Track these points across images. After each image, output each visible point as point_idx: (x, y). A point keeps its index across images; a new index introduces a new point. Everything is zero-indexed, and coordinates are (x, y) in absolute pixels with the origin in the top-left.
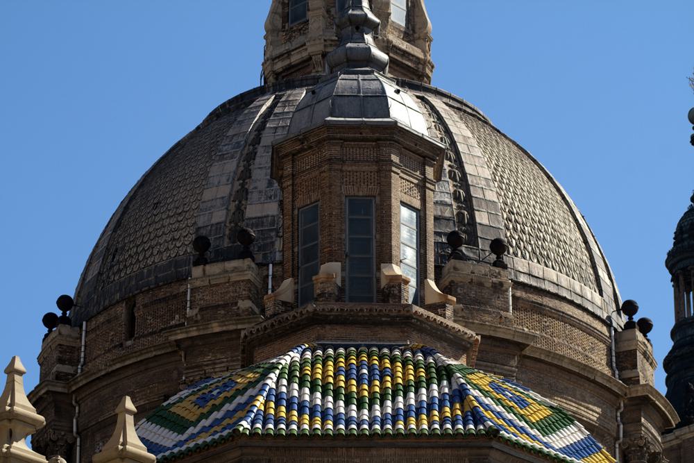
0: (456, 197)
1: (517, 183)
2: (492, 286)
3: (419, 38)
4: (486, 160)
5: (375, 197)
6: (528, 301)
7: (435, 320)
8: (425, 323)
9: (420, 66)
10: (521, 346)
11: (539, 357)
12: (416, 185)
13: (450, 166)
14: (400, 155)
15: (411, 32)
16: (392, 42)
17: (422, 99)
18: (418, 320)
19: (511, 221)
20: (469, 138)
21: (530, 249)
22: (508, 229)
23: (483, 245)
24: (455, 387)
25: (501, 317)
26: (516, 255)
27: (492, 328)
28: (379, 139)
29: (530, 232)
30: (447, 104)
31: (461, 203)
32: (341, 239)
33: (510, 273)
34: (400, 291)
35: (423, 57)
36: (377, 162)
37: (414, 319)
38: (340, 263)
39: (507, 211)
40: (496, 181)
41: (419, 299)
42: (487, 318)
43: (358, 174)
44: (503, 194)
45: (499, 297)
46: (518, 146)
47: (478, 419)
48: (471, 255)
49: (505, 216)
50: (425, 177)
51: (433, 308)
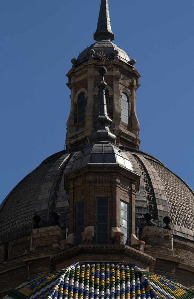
0: (149, 198)
1: (176, 192)
2: (164, 238)
3: (134, 129)
4: (162, 182)
5: (109, 197)
6: (180, 244)
7: (135, 251)
8: (130, 253)
9: (134, 141)
10: (177, 264)
11: (184, 268)
12: (128, 192)
13: (146, 185)
14: (120, 179)
15: (130, 127)
16: (122, 131)
17: (135, 155)
18: (127, 252)
19: (173, 209)
20: (155, 172)
21: (181, 221)
22: (171, 212)
23: (160, 219)
24: (143, 281)
25: (168, 251)
26: (175, 224)
27: (164, 256)
28: (111, 172)
30: (145, 158)
31: (151, 201)
32: (94, 216)
33: (172, 232)
34: (120, 239)
35: (135, 137)
36: (110, 182)
37: (126, 251)
38: (93, 227)
39: (171, 204)
40: (166, 191)
41: (128, 242)
42: (162, 251)
44: (169, 197)
45: (167, 242)
46: (177, 176)
48: (155, 224)
49: (170, 207)
50: (132, 189)
51: (135, 246)
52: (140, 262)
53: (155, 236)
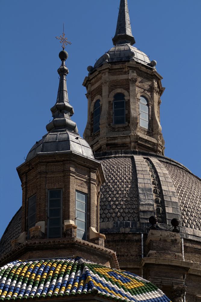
0: (156, 201)
1: (190, 193)
2: (171, 241)
3: (155, 134)
4: (175, 183)
5: (62, 188)
6: (192, 248)
7: (88, 244)
8: (83, 246)
9: (155, 147)
10: (187, 269)
11: (197, 274)
12: (85, 182)
13: (154, 187)
14: (75, 167)
15: (151, 131)
16: (139, 136)
17: (148, 159)
18: (78, 245)
19: (185, 211)
20: (166, 174)
21: (195, 223)
22: (183, 215)
23: (169, 223)
24: (84, 272)
25: (176, 256)
26: (187, 227)
27: (169, 261)
28: (64, 161)
29: (196, 216)
30: (159, 161)
31: (159, 204)
32: (45, 210)
33: (184, 235)
34: (71, 232)
35: (156, 142)
36: (63, 172)
37: (77, 244)
38: (44, 222)
39: (183, 206)
40: (179, 193)
41: (86, 237)
42: (169, 256)
43: (78, 185)
44: (182, 199)
45: (175, 246)
46: (196, 177)
47: (90, 286)
48: (163, 228)
49: (182, 209)
50: (90, 178)
52: (96, 257)
53: (160, 240)
